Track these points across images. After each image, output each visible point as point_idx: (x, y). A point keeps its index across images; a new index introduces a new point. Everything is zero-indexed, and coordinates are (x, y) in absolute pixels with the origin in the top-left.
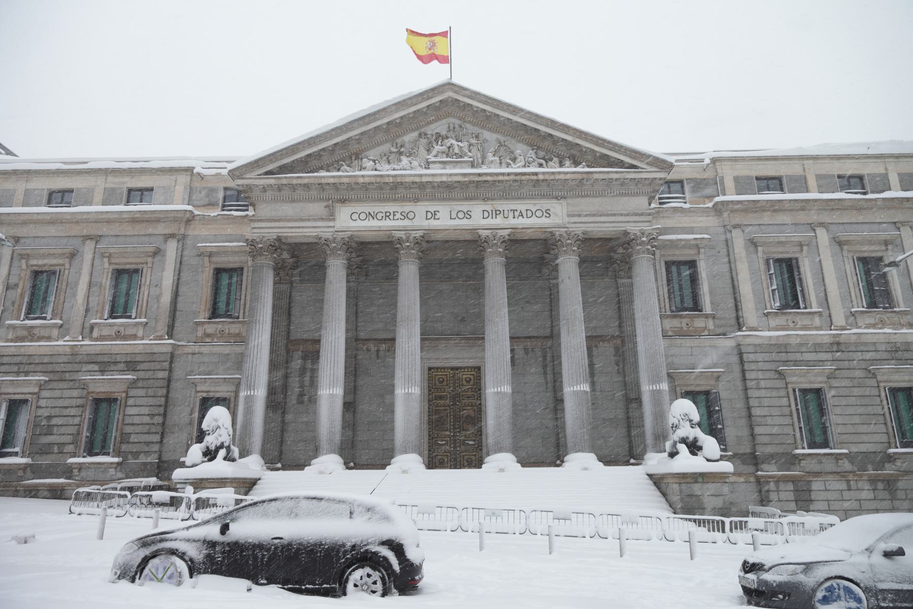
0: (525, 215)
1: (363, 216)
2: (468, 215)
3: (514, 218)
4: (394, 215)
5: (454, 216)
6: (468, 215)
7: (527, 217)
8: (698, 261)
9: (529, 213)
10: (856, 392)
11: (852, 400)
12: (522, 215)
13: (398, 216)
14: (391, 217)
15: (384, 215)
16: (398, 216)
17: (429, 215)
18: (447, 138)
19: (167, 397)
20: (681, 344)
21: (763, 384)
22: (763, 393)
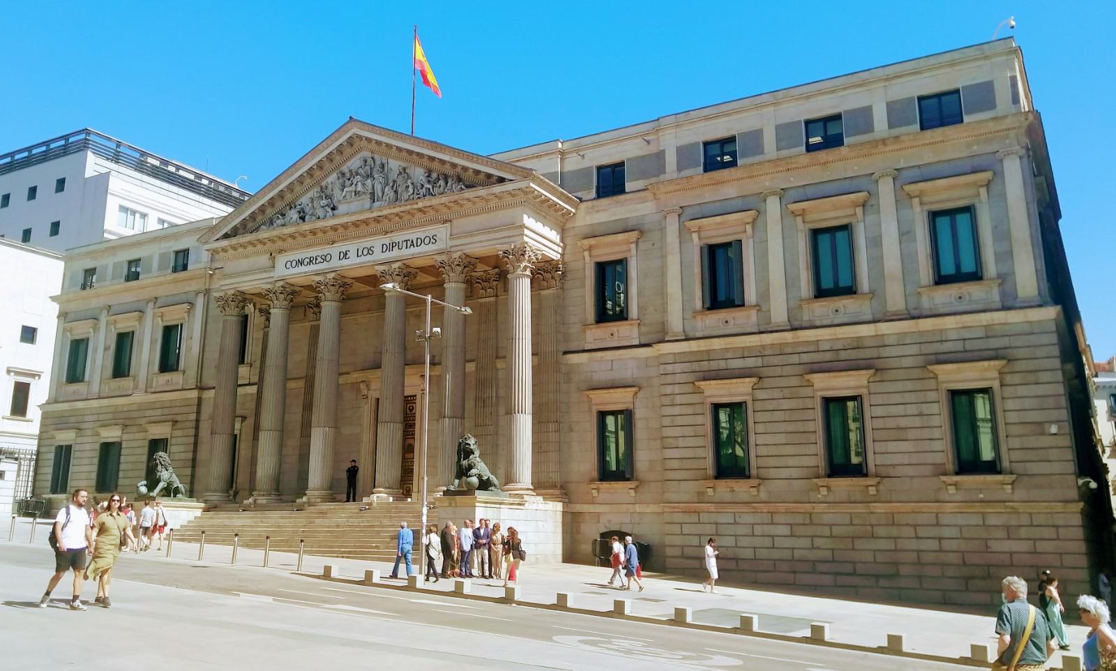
0: (415, 245)
1: (294, 263)
2: (370, 251)
3: (407, 248)
4: (316, 259)
5: (360, 253)
6: (370, 251)
7: (417, 246)
8: (629, 259)
9: (419, 241)
10: (786, 404)
11: (779, 416)
12: (413, 245)
13: (319, 259)
14: (314, 262)
15: (309, 260)
16: (319, 259)
17: (342, 255)
18: (357, 174)
19: (196, 436)
20: (601, 358)
21: (678, 399)
22: (677, 410)
